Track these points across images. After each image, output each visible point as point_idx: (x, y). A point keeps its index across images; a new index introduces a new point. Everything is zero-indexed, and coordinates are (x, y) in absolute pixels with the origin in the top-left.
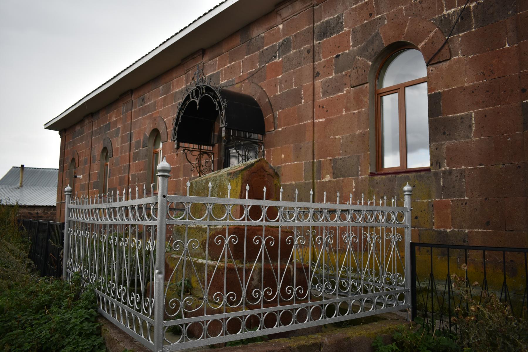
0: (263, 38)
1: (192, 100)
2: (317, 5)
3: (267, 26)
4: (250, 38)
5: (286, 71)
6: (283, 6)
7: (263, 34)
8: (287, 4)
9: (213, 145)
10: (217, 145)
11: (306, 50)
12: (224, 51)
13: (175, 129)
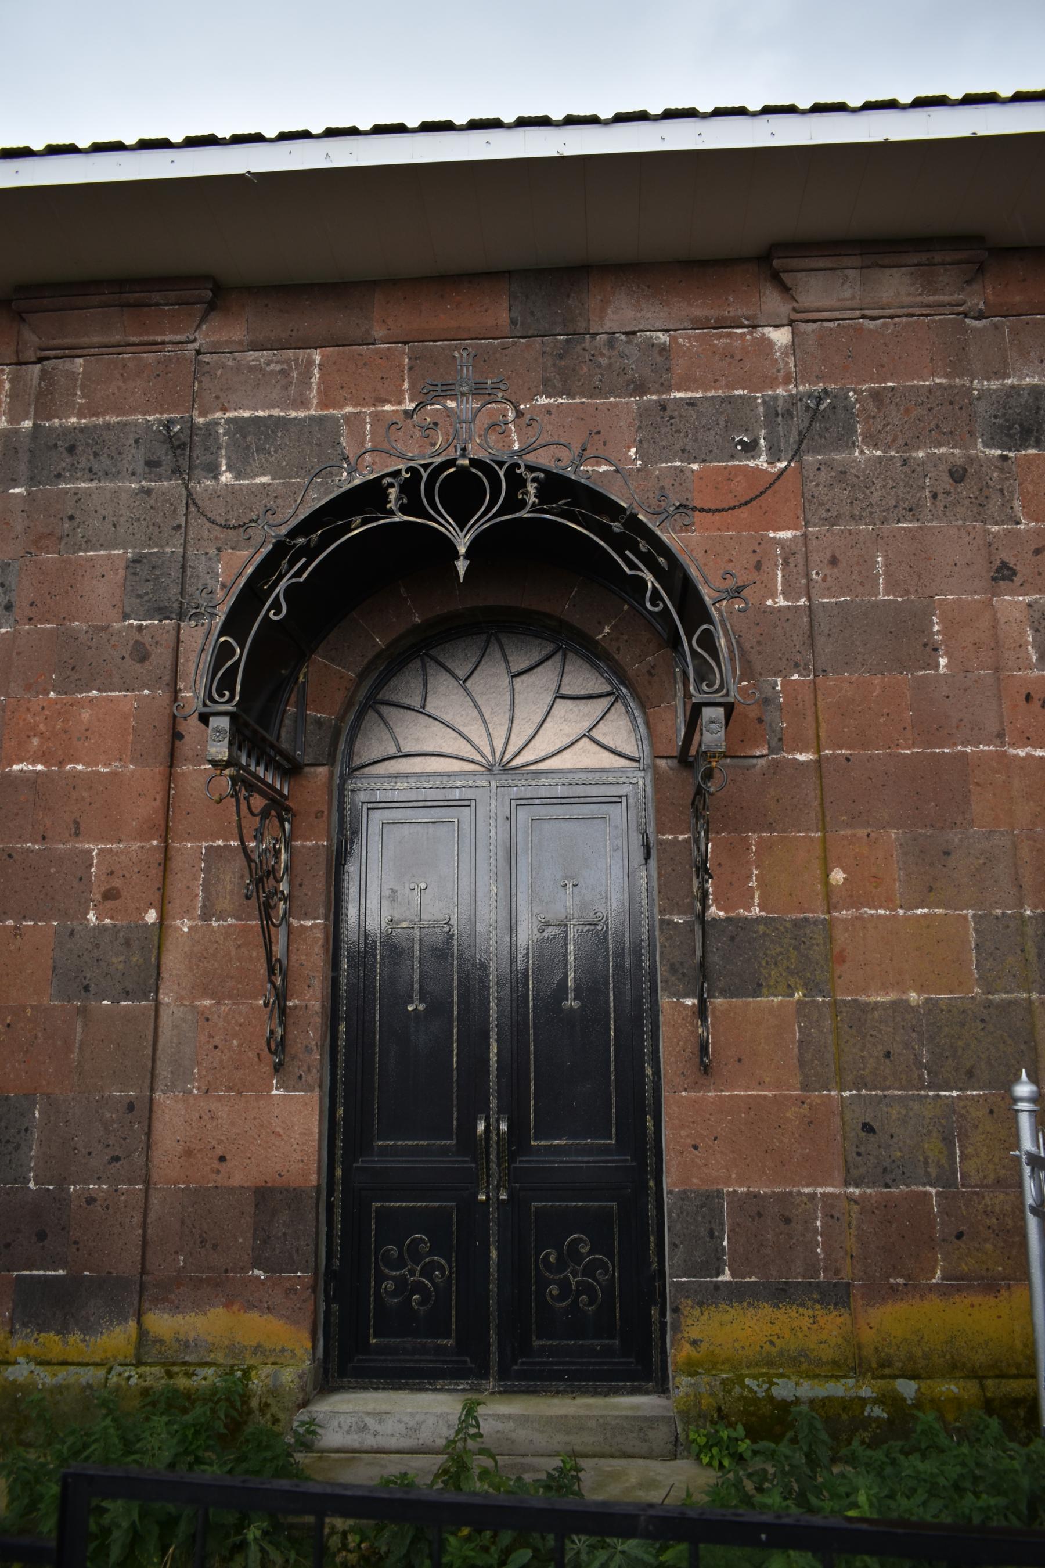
0: (663, 349)
1: (400, 518)
2: (980, 316)
3: (699, 312)
4: (581, 326)
5: (833, 521)
6: (821, 263)
7: (663, 337)
8: (847, 261)
9: (292, 770)
10: (323, 770)
11: (943, 467)
12: (378, 332)
13: (224, 652)
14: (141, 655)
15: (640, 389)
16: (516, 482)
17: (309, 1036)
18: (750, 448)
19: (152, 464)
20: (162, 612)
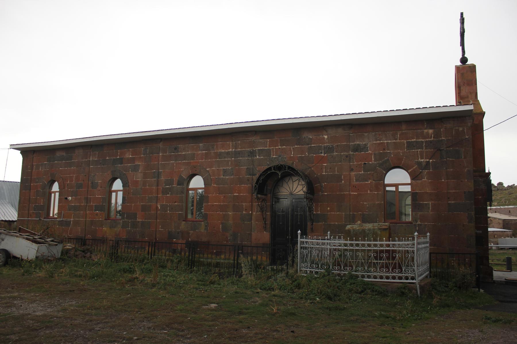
0: (311, 139)
9: (266, 195)
13: (256, 186)
14: (248, 180)
15: (308, 145)
16: (285, 167)
17: (268, 226)
18: (321, 153)
19: (249, 155)
20: (250, 175)
